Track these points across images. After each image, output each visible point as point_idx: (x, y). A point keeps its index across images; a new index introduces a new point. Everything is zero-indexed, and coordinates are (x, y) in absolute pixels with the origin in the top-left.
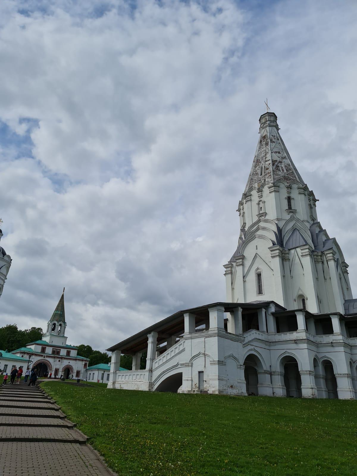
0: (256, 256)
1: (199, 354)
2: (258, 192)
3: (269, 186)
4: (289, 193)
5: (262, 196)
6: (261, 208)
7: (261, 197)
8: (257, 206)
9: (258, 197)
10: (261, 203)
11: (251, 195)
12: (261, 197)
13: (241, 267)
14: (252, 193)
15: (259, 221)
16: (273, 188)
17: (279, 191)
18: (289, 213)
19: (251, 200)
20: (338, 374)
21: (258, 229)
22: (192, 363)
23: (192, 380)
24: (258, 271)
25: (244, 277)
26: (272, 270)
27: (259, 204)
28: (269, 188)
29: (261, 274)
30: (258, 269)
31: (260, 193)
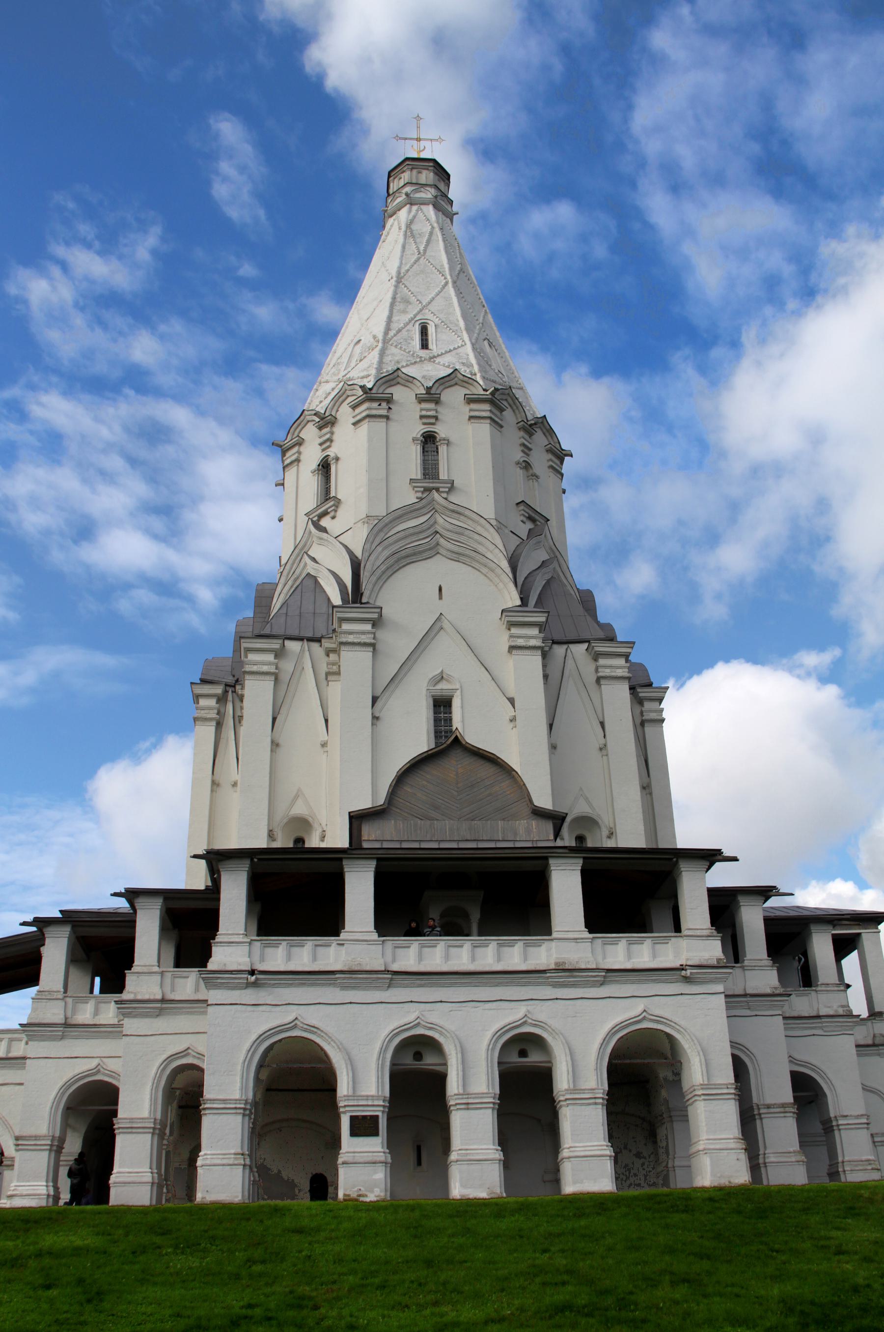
0: (436, 628)
3: (468, 392)
4: (526, 449)
5: (436, 418)
7: (433, 421)
9: (422, 417)
11: (389, 400)
12: (433, 421)
13: (366, 655)
14: (398, 393)
16: (487, 407)
17: (502, 427)
18: (525, 519)
19: (387, 418)
20: (768, 1107)
25: (375, 700)
31: (431, 406)
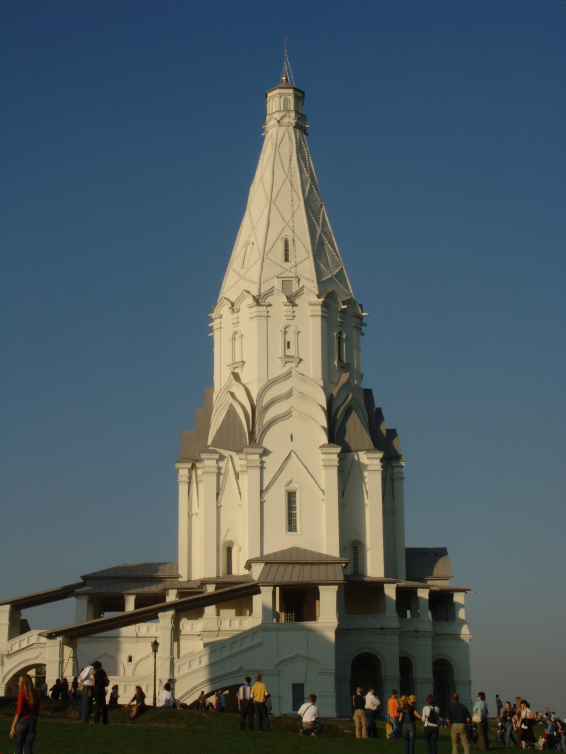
1: (297, 656)
2: (285, 305)
6: (289, 343)
8: (280, 337)
10: (287, 330)
15: (288, 375)
21: (289, 394)
22: (279, 671)
23: (280, 697)
24: (290, 486)
26: (323, 491)
27: (286, 332)
28: (311, 305)
29: (294, 493)
30: (291, 482)
31: (290, 308)
